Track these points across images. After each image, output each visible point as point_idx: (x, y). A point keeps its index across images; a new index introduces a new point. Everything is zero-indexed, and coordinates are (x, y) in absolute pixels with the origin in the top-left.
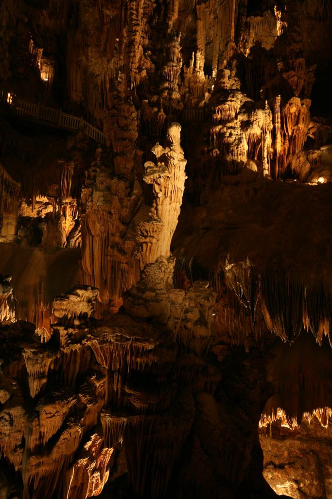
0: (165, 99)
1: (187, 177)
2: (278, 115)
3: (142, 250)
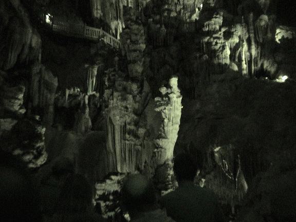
0: (165, 17)
1: (182, 107)
2: (252, 27)
3: (155, 155)
